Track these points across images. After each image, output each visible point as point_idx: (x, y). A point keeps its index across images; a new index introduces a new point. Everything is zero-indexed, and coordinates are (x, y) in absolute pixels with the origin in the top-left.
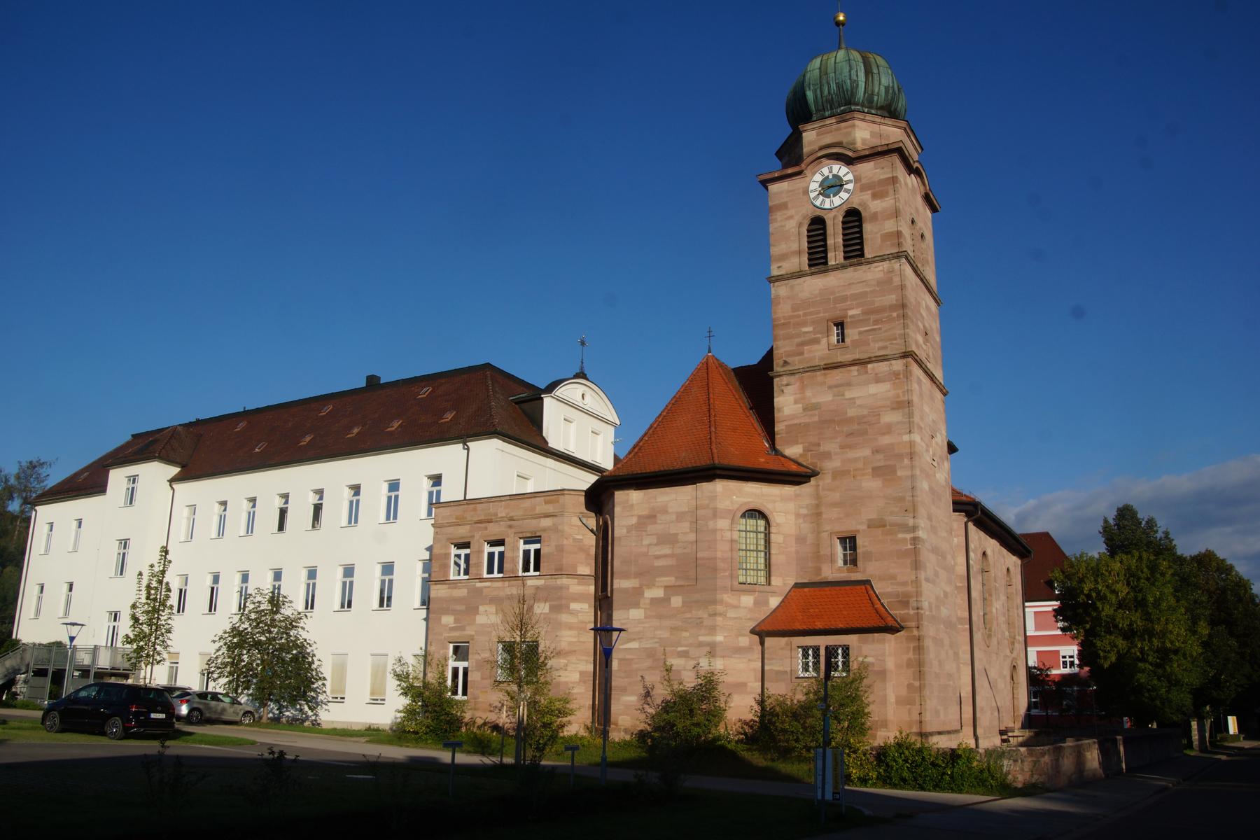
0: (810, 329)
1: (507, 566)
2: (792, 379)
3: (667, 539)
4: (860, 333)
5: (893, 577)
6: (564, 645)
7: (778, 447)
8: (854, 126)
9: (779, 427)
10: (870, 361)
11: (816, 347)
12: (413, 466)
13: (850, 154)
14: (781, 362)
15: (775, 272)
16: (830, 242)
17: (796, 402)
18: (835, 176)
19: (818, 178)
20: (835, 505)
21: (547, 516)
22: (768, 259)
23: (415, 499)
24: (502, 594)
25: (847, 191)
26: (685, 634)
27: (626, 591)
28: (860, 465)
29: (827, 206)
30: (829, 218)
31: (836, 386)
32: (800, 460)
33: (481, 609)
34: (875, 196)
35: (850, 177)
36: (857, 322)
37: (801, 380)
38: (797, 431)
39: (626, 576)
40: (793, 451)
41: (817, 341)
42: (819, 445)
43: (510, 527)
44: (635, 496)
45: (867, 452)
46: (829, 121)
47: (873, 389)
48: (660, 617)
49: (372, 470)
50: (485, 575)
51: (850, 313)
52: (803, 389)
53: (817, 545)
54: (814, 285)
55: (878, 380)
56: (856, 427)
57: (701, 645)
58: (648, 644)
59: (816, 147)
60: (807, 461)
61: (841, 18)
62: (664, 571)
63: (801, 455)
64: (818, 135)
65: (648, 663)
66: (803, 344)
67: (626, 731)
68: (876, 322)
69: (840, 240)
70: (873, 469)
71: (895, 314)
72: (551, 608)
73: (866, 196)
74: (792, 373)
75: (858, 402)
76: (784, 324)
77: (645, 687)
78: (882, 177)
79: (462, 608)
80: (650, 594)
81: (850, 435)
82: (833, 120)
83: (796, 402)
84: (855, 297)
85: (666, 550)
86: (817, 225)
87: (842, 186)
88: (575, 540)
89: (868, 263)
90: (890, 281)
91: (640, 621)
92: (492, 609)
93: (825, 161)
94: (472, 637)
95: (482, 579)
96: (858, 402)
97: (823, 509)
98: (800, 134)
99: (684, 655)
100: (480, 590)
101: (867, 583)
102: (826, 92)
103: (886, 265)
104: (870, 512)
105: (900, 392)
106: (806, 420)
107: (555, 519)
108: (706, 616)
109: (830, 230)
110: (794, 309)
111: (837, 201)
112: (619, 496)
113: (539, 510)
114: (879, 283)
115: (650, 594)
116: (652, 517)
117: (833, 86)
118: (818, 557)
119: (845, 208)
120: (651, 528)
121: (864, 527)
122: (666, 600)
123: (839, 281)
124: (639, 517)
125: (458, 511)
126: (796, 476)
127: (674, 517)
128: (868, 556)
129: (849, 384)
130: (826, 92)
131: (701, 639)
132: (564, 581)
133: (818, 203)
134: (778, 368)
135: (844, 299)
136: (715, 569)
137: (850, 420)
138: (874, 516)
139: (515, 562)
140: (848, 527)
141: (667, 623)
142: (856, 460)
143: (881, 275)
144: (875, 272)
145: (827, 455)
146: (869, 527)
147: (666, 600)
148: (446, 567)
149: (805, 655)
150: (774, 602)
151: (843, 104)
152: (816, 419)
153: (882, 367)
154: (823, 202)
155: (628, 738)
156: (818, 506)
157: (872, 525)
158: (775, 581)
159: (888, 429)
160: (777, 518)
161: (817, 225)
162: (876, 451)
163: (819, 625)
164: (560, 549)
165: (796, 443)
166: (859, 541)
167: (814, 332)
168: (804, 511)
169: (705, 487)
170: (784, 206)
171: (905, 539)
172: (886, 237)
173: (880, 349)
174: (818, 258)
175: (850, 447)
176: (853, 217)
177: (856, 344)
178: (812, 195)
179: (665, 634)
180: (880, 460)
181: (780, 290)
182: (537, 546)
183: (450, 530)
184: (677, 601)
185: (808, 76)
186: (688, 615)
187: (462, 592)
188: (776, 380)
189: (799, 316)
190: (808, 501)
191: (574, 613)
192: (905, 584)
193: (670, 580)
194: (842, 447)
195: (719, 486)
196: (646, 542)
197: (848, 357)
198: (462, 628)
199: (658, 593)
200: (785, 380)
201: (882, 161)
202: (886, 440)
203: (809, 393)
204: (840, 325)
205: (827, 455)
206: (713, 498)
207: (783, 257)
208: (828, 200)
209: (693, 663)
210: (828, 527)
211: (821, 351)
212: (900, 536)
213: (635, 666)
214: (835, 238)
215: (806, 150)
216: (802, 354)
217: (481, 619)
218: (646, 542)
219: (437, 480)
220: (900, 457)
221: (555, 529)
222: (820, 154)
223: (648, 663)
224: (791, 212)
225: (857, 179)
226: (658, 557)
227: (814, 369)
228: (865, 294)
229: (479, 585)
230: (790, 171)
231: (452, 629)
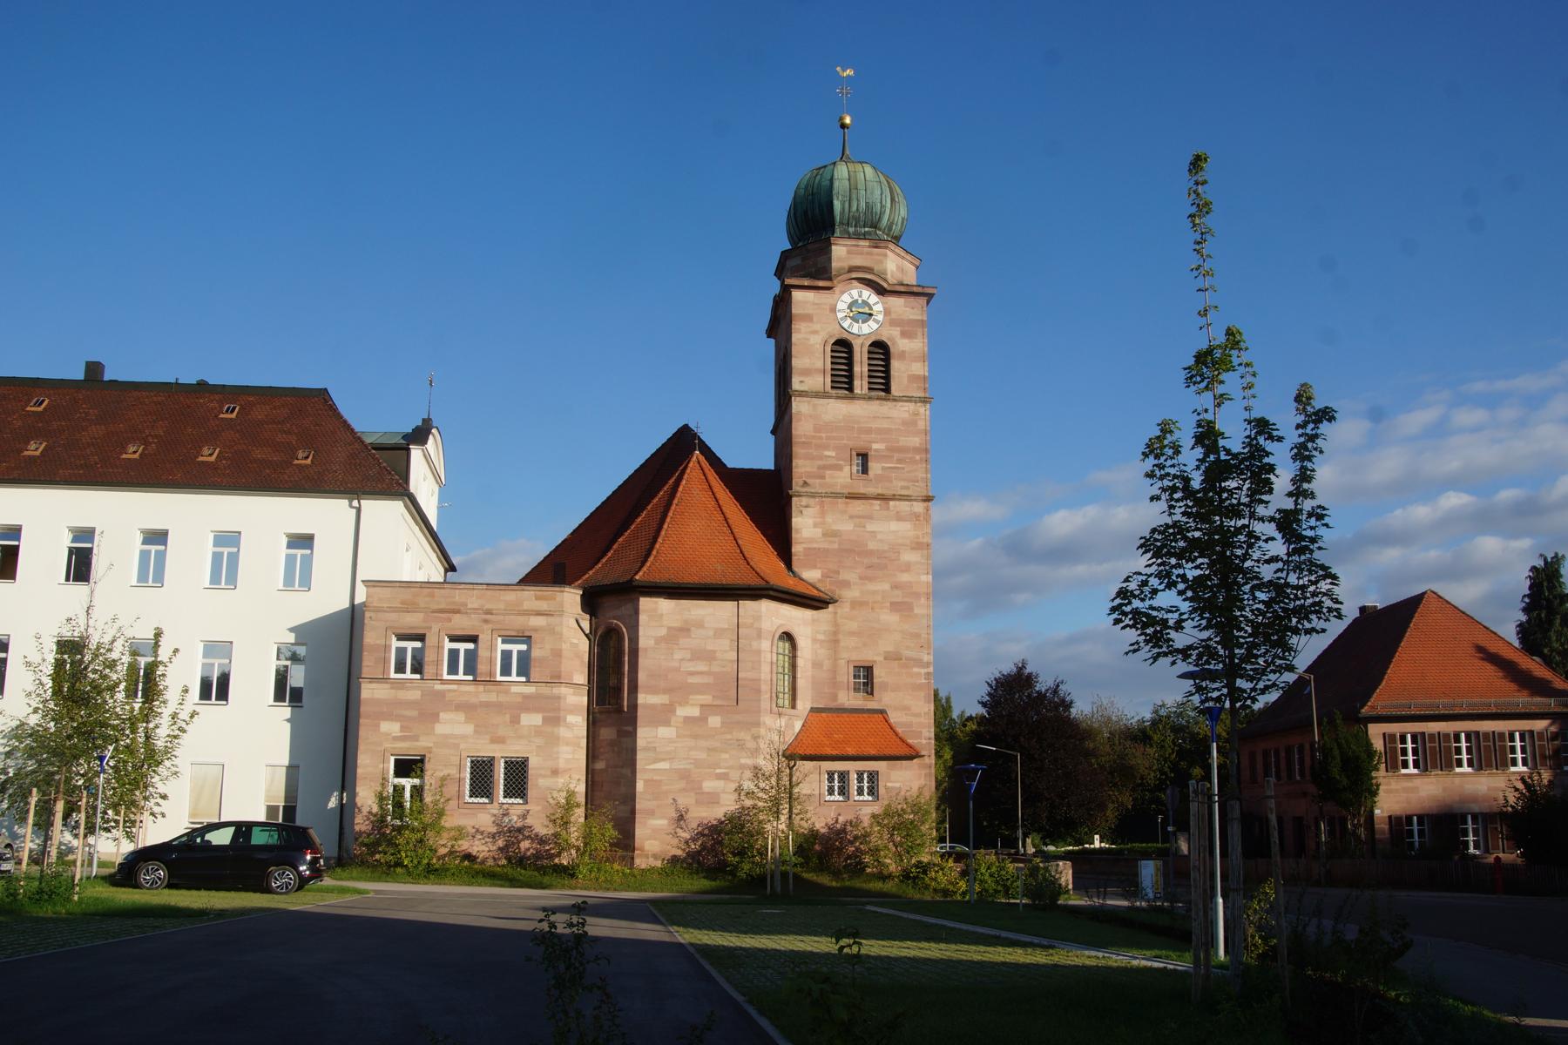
1: (482, 667)
2: (812, 501)
3: (709, 656)
5: (906, 708)
6: (562, 764)
7: (795, 568)
9: (797, 549)
10: (894, 498)
11: (837, 473)
12: (265, 518)
16: (857, 369)
17: (815, 525)
19: (846, 298)
20: (852, 634)
21: (539, 613)
23: (264, 555)
24: (474, 700)
27: (653, 707)
28: (879, 598)
29: (855, 330)
30: (856, 344)
32: (819, 585)
33: (442, 715)
34: (904, 334)
36: (882, 458)
37: (822, 504)
38: (815, 556)
39: (654, 690)
40: (811, 575)
41: (840, 468)
43: (486, 621)
44: (664, 605)
45: (886, 586)
46: (862, 243)
47: (894, 526)
48: (695, 737)
49: (193, 516)
50: (446, 677)
51: (875, 446)
52: (823, 513)
53: (834, 671)
54: (837, 409)
55: (899, 518)
56: (876, 561)
58: (677, 765)
59: (846, 265)
60: (826, 588)
61: (848, 120)
62: (699, 688)
64: (849, 252)
65: (682, 784)
66: (825, 467)
67: (655, 857)
68: (900, 461)
69: (866, 369)
72: (544, 719)
74: (813, 495)
77: (677, 810)
79: (415, 713)
80: (682, 712)
81: (869, 567)
82: (867, 243)
83: (815, 525)
84: (880, 431)
86: (843, 346)
90: (914, 423)
91: (671, 741)
92: (461, 717)
93: (855, 283)
94: (429, 750)
95: (443, 682)
97: (840, 637)
98: (830, 245)
99: (724, 777)
100: (442, 694)
101: (882, 712)
102: (854, 208)
103: (911, 406)
104: (887, 644)
106: (826, 546)
107: (550, 619)
109: (857, 357)
110: (817, 429)
112: (645, 603)
113: (527, 605)
114: (904, 423)
115: (682, 712)
116: (685, 630)
117: (863, 205)
118: (834, 683)
120: (683, 642)
121: (879, 659)
122: (702, 719)
123: (861, 412)
124: (669, 628)
125: (406, 595)
126: (814, 602)
127: (711, 633)
128: (885, 686)
129: (870, 517)
130: (854, 208)
131: (743, 761)
132: (563, 690)
133: (845, 325)
134: (797, 486)
135: (869, 431)
136: (758, 691)
137: (871, 553)
138: (890, 649)
139: (491, 661)
140: (866, 656)
141: (703, 743)
142: (875, 593)
143: (906, 415)
144: (902, 411)
145: (846, 584)
147: (702, 719)
148: (386, 661)
149: (831, 779)
150: (798, 725)
151: (870, 227)
152: (836, 546)
153: (904, 506)
155: (659, 864)
156: (835, 633)
158: (799, 704)
159: (907, 568)
160: (803, 644)
161: (843, 346)
162: (895, 587)
163: (851, 751)
164: (558, 654)
165: (815, 567)
166: (876, 672)
168: (821, 637)
169: (747, 605)
170: (808, 318)
172: (913, 378)
174: (843, 380)
176: (880, 349)
177: (880, 478)
178: (840, 315)
179: (703, 756)
180: (898, 596)
182: (524, 647)
183: (393, 616)
185: (836, 184)
187: (414, 695)
188: (794, 500)
190: (825, 627)
191: (570, 726)
192: (918, 715)
193: (706, 699)
195: (766, 606)
196: (678, 655)
197: (871, 490)
198: (415, 738)
200: (804, 501)
201: (912, 299)
202: (905, 578)
203: (829, 519)
204: (864, 457)
205: (846, 584)
206: (758, 618)
207: (807, 372)
209: (734, 786)
210: (845, 655)
212: (915, 670)
214: (861, 367)
215: (834, 265)
216: (823, 477)
217: (440, 729)
218: (678, 655)
220: (917, 595)
221: (551, 630)
222: (854, 275)
223: (682, 784)
224: (817, 327)
225: (887, 312)
226: (692, 674)
227: (836, 495)
228: (888, 431)
229: (438, 687)
230: (821, 283)
231: (395, 739)
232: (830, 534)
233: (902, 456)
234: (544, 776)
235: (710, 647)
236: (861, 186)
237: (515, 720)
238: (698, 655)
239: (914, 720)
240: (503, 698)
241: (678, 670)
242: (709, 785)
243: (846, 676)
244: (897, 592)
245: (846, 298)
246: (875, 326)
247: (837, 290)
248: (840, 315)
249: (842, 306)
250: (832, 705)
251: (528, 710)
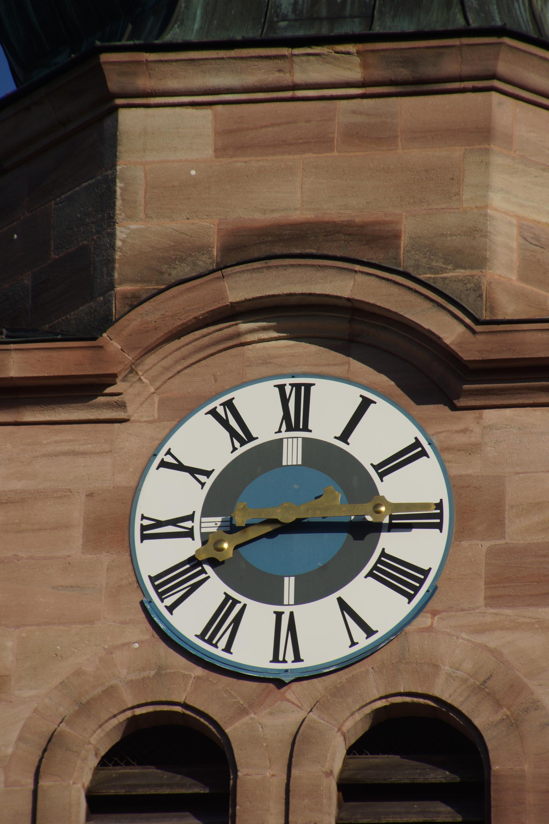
8: (482, 134)
13: (449, 331)
18: (328, 460)
19: (203, 442)
25: (399, 576)
29: (252, 647)
30: (257, 737)
46: (314, 67)
59: (205, 225)
64: (231, 143)
82: (342, 66)
87: (364, 531)
98: (103, 108)
111: (323, 634)
119: (373, 690)
133: (190, 619)
154: (226, 620)
208: (258, 617)
215: (134, 231)
222: (241, 287)
225: (471, 509)
245: (203, 442)
247: (137, 394)
248: (156, 557)
249: (167, 495)
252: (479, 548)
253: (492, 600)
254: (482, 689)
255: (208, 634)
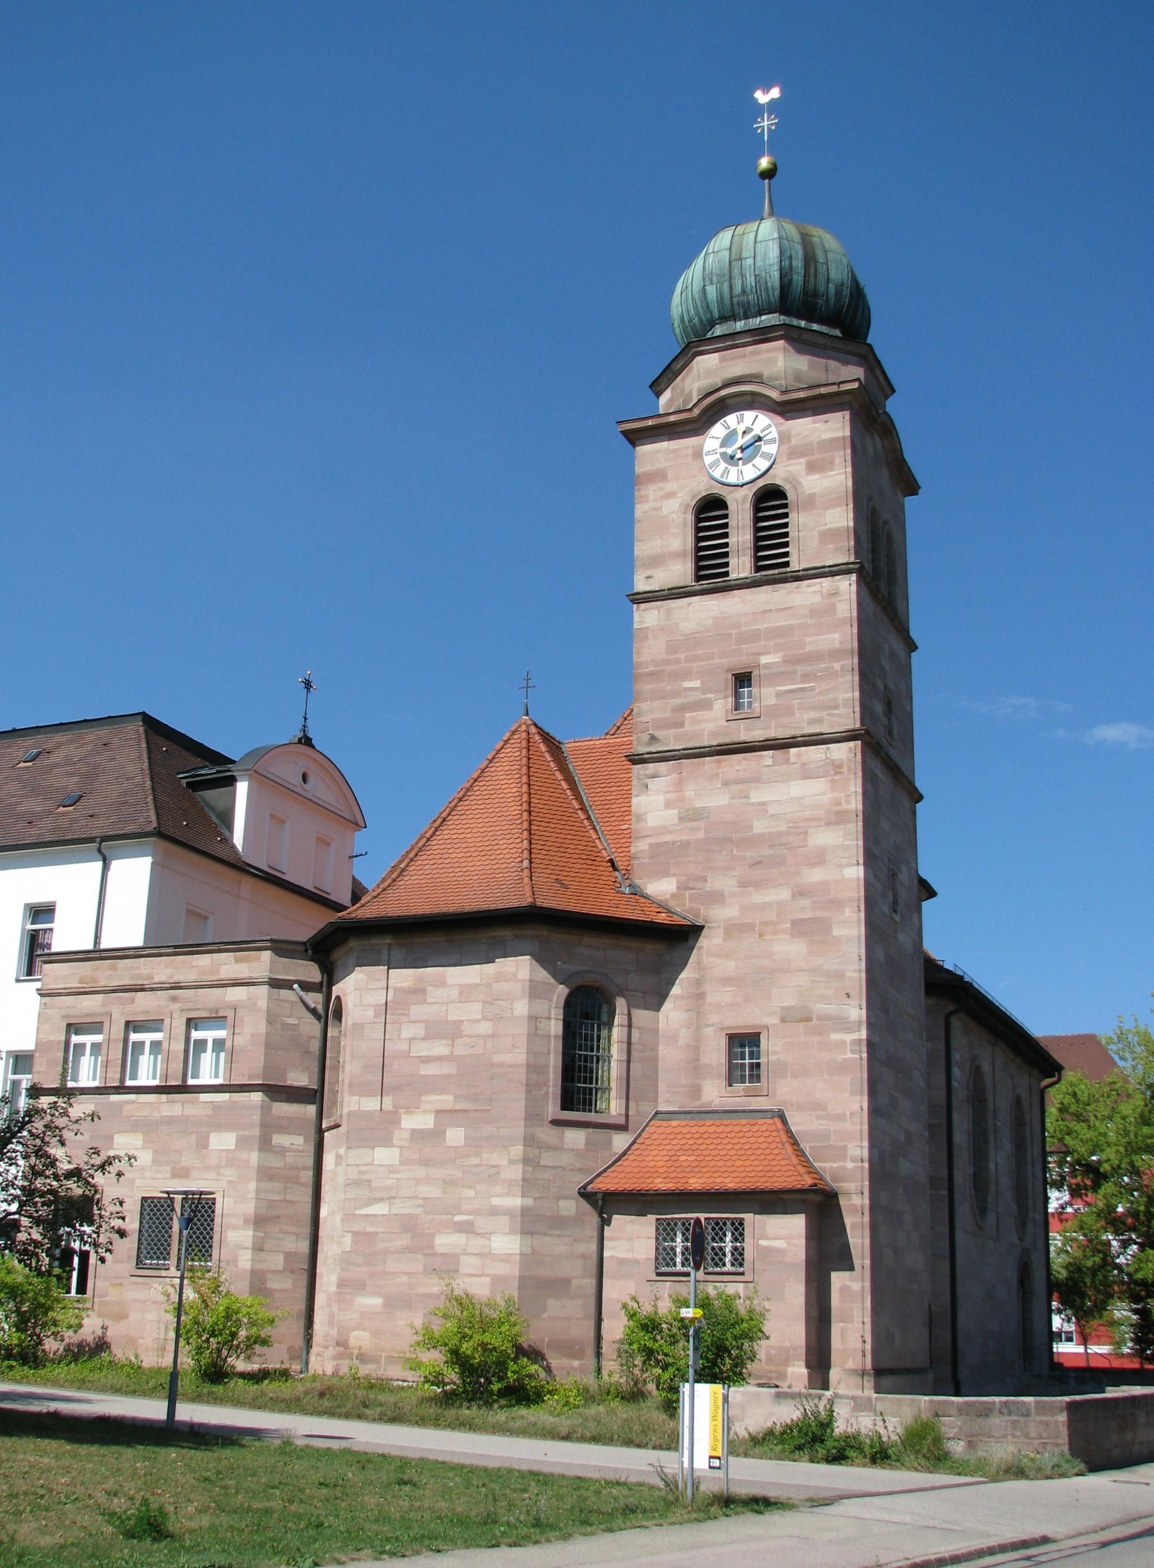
0: (696, 684)
2: (662, 767)
4: (779, 694)
5: (819, 1107)
11: (703, 714)
14: (645, 737)
15: (641, 585)
17: (668, 805)
22: (627, 563)
25: (766, 456)
26: (470, 1193)
28: (772, 916)
29: (732, 479)
31: (737, 782)
34: (812, 468)
35: (774, 433)
38: (667, 855)
40: (660, 888)
41: (707, 705)
42: (704, 879)
43: (174, 999)
45: (784, 894)
47: (798, 789)
48: (426, 1163)
51: (764, 660)
56: (768, 852)
57: (494, 1212)
59: (718, 381)
63: (673, 896)
64: (722, 360)
65: (404, 1240)
66: (683, 708)
68: (806, 677)
70: (794, 923)
71: (837, 666)
73: (798, 467)
75: (772, 810)
76: (652, 674)
78: (824, 436)
80: (411, 1122)
81: (756, 864)
83: (668, 805)
84: (774, 633)
85: (440, 1048)
88: (283, 1024)
89: (797, 578)
90: (832, 609)
91: (391, 1169)
96: (772, 810)
97: (707, 988)
99: (466, 1228)
102: (738, 289)
103: (826, 582)
104: (784, 996)
105: (842, 795)
106: (685, 837)
108: (506, 1162)
110: (672, 648)
111: (749, 472)
114: (814, 612)
115: (411, 1122)
120: (416, 1011)
122: (438, 1133)
127: (455, 993)
129: (756, 780)
130: (738, 289)
131: (496, 1201)
133: (717, 474)
135: (754, 636)
137: (759, 840)
138: (790, 1001)
142: (765, 906)
143: (817, 599)
145: (717, 897)
146: (783, 1020)
147: (438, 1133)
152: (701, 835)
153: (815, 753)
154: (726, 472)
157: (787, 1017)
159: (820, 858)
162: (799, 893)
165: (666, 874)
167: (703, 690)
170: (659, 476)
171: (843, 1042)
173: (812, 722)
175: (757, 885)
178: (708, 460)
179: (434, 1192)
180: (804, 909)
181: (647, 617)
184: (455, 1136)
186: (475, 1161)
189: (678, 661)
192: (839, 1118)
193: (446, 1100)
194: (743, 884)
197: (757, 734)
199: (425, 1121)
202: (816, 875)
203: (689, 792)
205: (717, 897)
207: (657, 561)
208: (733, 470)
210: (714, 1018)
211: (713, 722)
212: (834, 1036)
213: (381, 1246)
216: (681, 724)
218: (407, 1032)
219: (41, 912)
220: (838, 904)
223: (404, 1240)
224: (670, 486)
225: (784, 438)
226: (426, 1060)
228: (791, 628)
232: (691, 816)
233: (808, 669)
234: (235, 1227)
235: (451, 1018)
236: (747, 253)
237: (203, 1144)
238: (437, 1030)
239: (834, 1126)
240: (190, 1110)
241: (407, 1055)
242: (445, 1242)
243: (716, 1053)
244: (805, 902)
246: (762, 464)
250: (692, 1106)
251: (220, 1127)
252: (785, 447)
253: (789, 459)
254: (786, 480)
255: (722, 476)
